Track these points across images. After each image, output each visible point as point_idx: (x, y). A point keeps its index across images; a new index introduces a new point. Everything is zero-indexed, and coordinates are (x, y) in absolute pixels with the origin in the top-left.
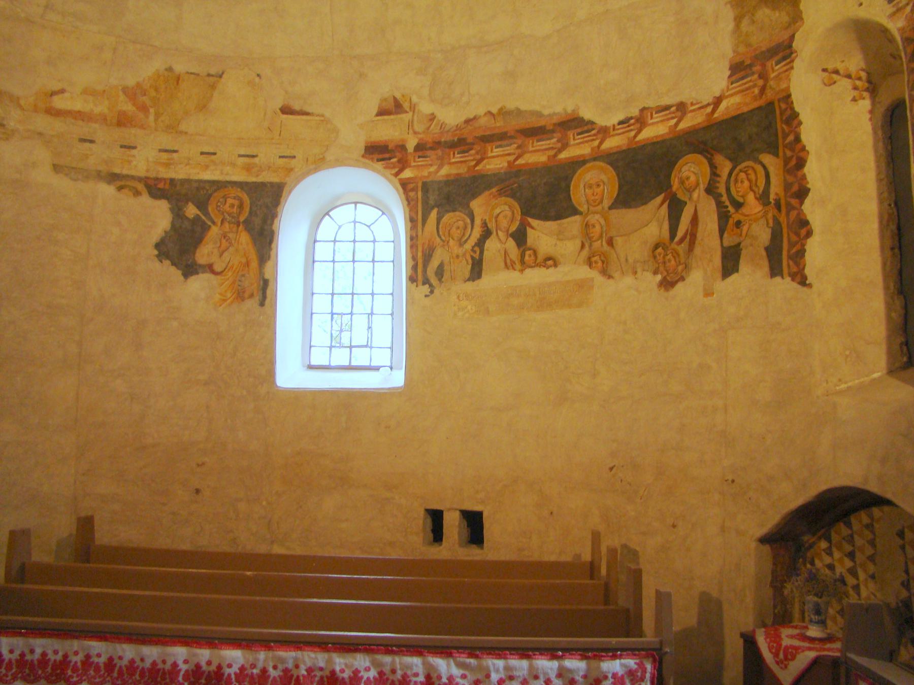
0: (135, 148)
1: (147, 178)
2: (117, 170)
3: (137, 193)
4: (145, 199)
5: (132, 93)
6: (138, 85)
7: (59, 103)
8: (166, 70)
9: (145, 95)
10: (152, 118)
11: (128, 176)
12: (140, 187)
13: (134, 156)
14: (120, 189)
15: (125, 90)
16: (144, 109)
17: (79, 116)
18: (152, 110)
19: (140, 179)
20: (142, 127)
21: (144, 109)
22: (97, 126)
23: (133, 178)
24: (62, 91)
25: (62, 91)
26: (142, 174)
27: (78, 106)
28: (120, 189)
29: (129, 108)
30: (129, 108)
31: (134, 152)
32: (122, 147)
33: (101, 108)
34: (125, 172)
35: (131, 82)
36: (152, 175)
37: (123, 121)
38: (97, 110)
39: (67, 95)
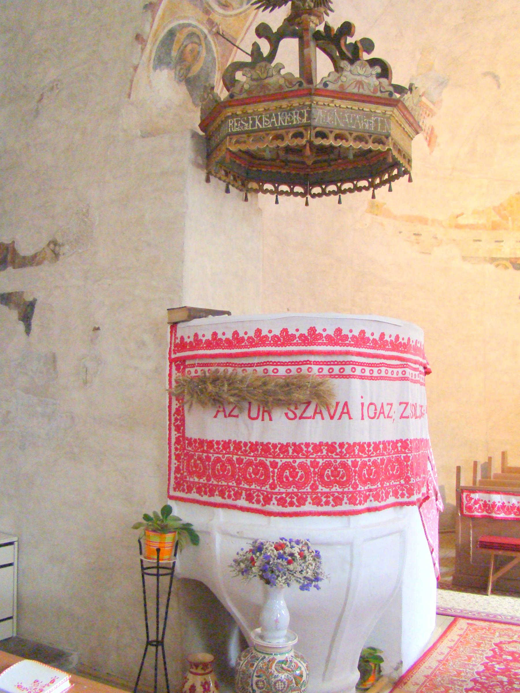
0: (502, 241)
1: (510, 258)
2: (494, 256)
3: (506, 268)
4: (511, 270)
5: (498, 210)
6: (501, 205)
7: (462, 221)
8: (516, 194)
9: (505, 210)
10: (510, 223)
11: (500, 258)
12: (508, 264)
13: (502, 246)
14: (497, 266)
15: (494, 208)
16: (505, 218)
17: (472, 227)
18: (510, 218)
19: (507, 259)
20: (505, 229)
21: (505, 218)
22: (481, 231)
23: (503, 259)
24: (462, 214)
25: (462, 214)
26: (508, 256)
27: (471, 221)
28: (497, 266)
29: (497, 218)
30: (497, 218)
31: (502, 244)
32: (496, 241)
33: (482, 221)
34: (499, 256)
35: (497, 204)
36: (513, 256)
37: (495, 227)
38: (480, 222)
39: (464, 216)
